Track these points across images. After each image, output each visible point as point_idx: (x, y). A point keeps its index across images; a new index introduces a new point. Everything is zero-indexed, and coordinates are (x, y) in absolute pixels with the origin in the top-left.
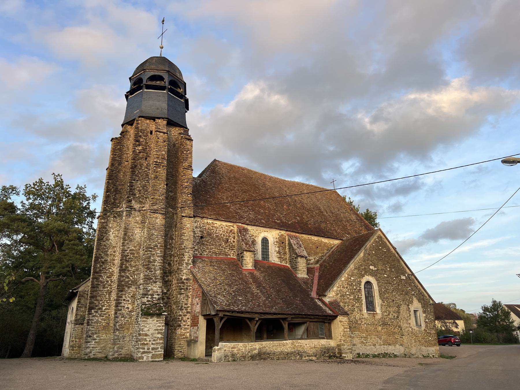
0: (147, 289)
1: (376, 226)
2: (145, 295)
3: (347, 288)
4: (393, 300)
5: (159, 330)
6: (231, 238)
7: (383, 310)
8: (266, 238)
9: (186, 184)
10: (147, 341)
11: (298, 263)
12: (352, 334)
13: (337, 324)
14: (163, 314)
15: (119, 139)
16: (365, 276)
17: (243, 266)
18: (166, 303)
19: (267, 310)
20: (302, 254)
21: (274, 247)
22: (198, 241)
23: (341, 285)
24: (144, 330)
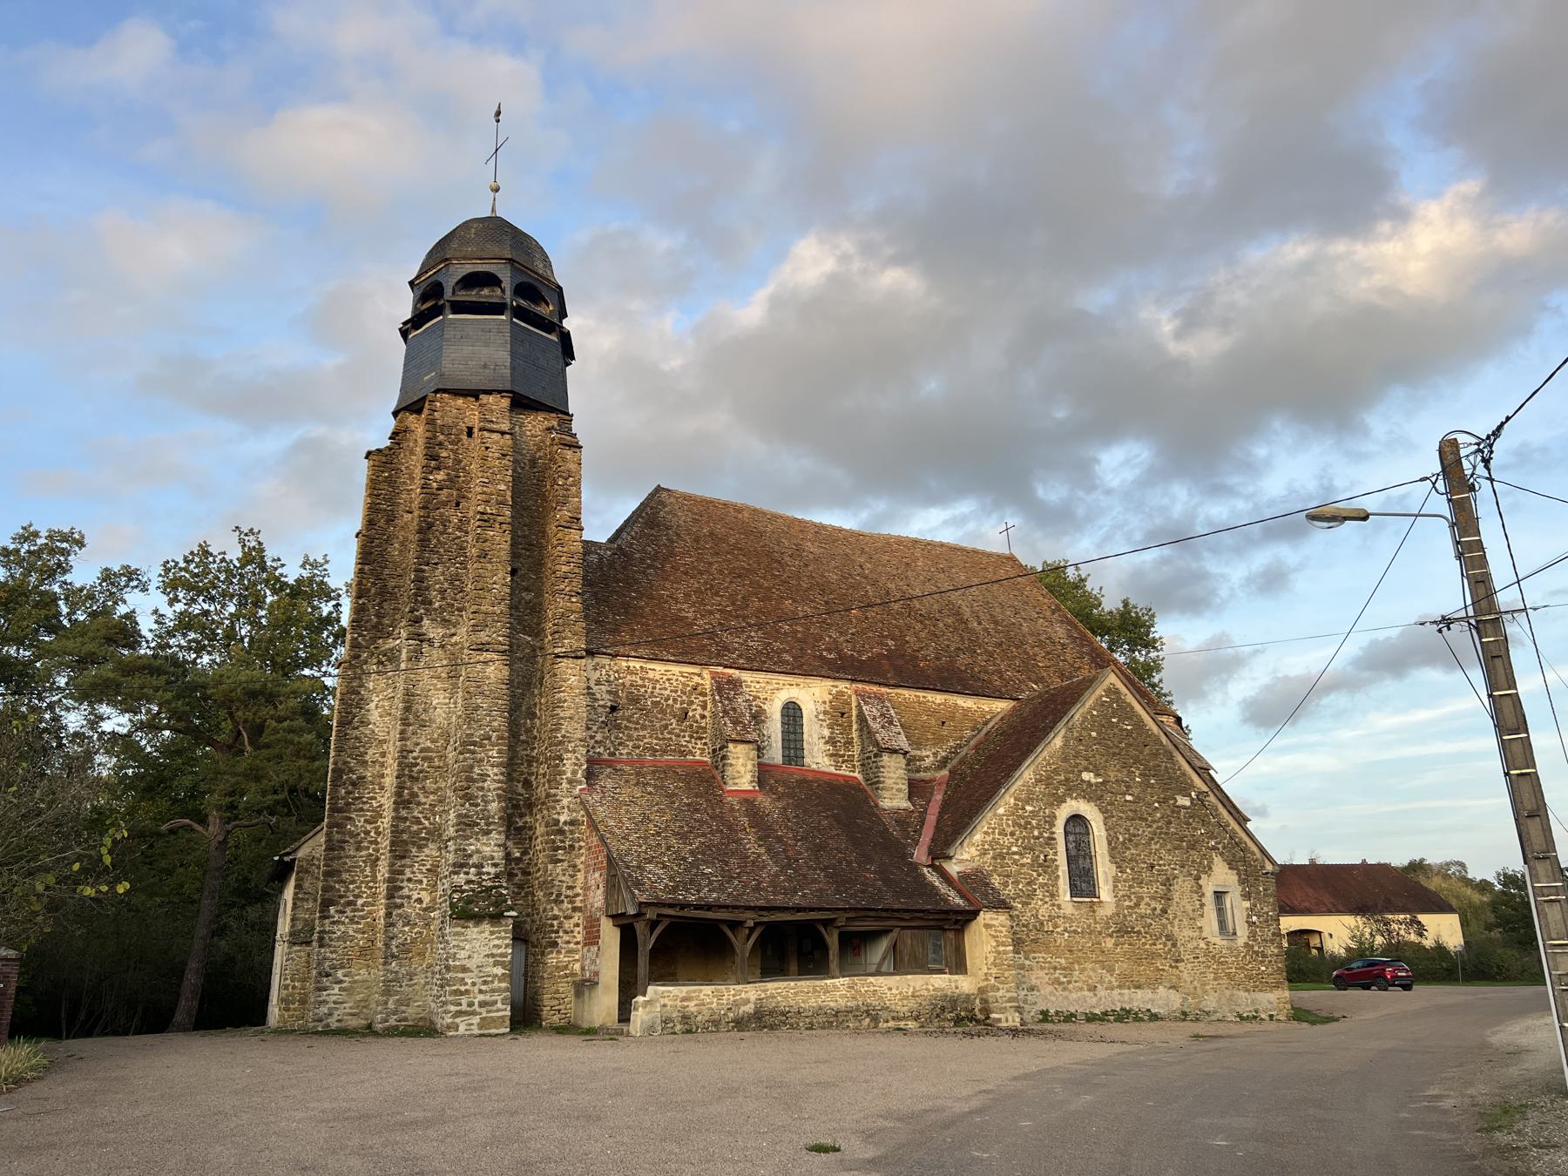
0: (465, 850)
1: (1154, 647)
2: (459, 866)
3: (1012, 834)
5: (497, 955)
7: (1121, 893)
9: (565, 569)
10: (466, 984)
11: (882, 770)
14: (505, 914)
15: (387, 452)
16: (1068, 800)
18: (520, 886)
19: (779, 900)
20: (895, 745)
21: (817, 726)
22: (603, 719)
24: (458, 956)
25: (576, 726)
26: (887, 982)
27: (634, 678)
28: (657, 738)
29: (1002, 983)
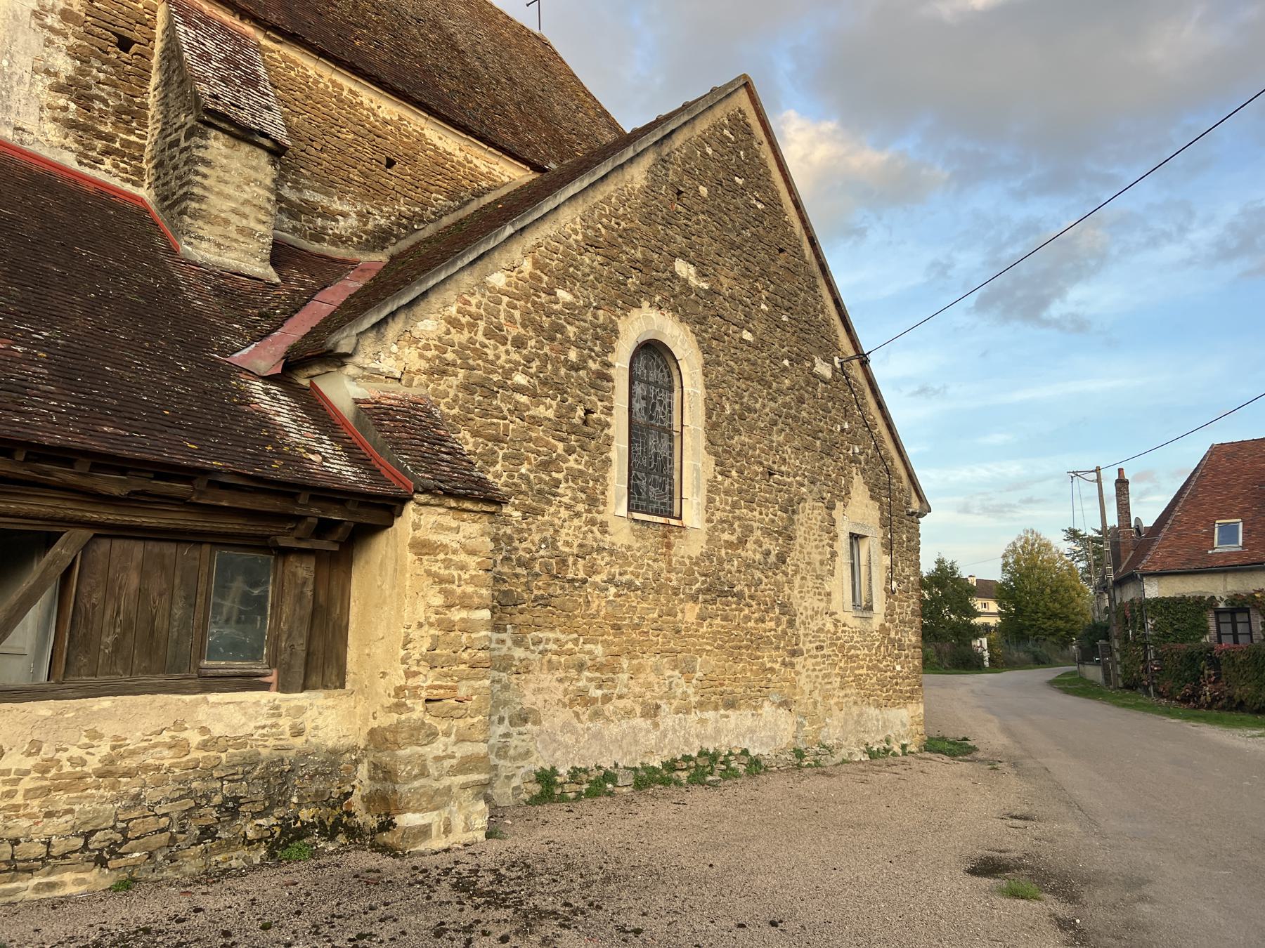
3: (519, 343)
4: (770, 468)
7: (719, 515)
11: (202, 169)
12: (518, 643)
13: (390, 566)
16: (645, 304)
23: (477, 318)
29: (447, 716)
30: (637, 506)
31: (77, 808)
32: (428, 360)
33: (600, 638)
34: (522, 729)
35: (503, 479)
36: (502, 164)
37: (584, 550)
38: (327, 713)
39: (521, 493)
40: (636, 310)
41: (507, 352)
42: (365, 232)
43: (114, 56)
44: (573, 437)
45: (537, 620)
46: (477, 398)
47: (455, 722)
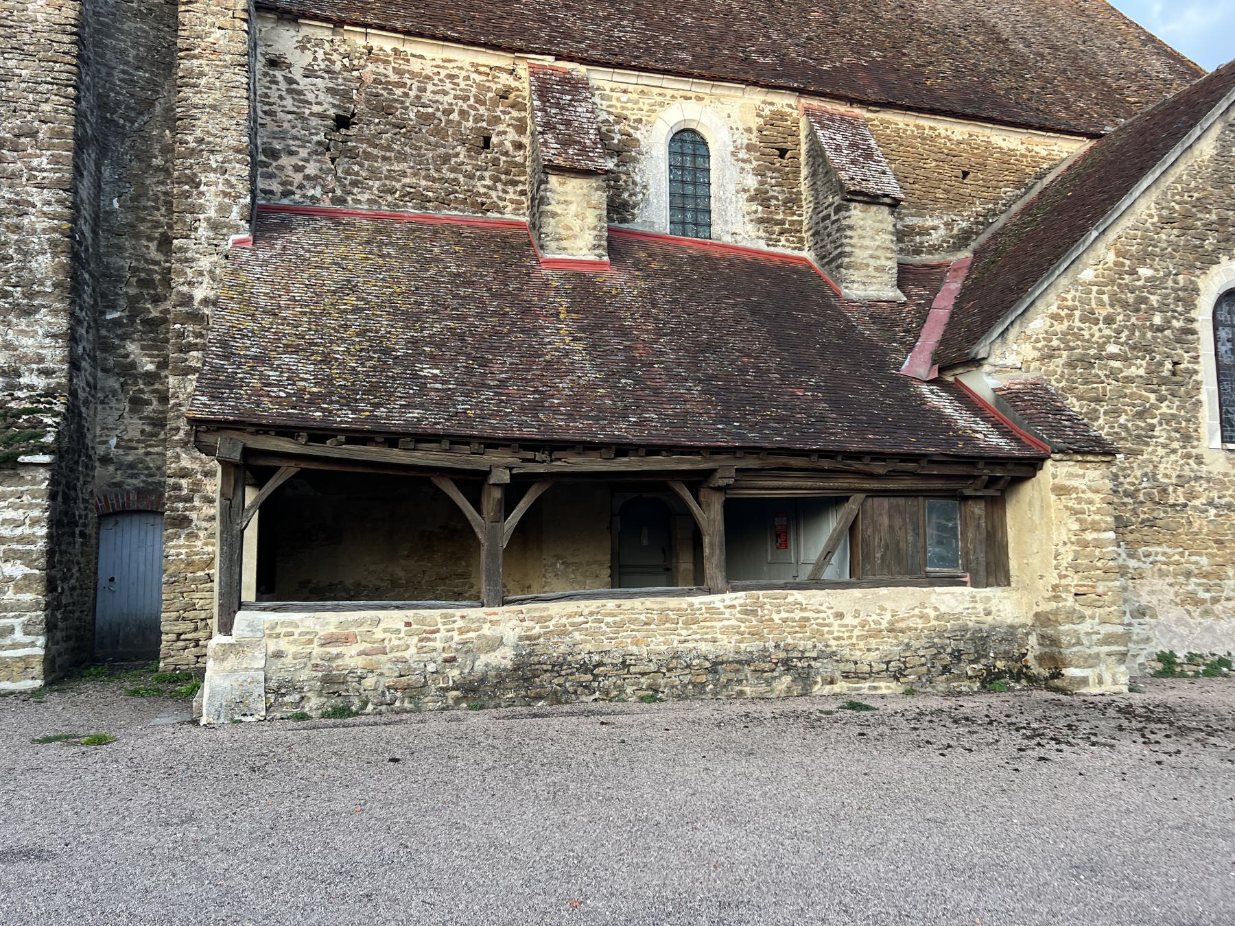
3: (1109, 320)
5: (11, 540)
6: (501, 128)
8: (693, 131)
11: (849, 233)
12: (1130, 556)
13: (1037, 504)
14: (24, 459)
16: (1224, 259)
17: (542, 247)
19: (579, 428)
20: (872, 188)
22: (321, 137)
25: (226, 122)
26: (830, 599)
27: (381, 69)
28: (427, 178)
30: (1231, 437)
31: (881, 647)
32: (1039, 350)
33: (1205, 551)
34: (1141, 621)
35: (1106, 430)
36: (1060, 143)
37: (1182, 479)
38: (1005, 601)
39: (1122, 439)
40: (1214, 266)
41: (1100, 330)
42: (951, 237)
43: (778, 165)
44: (1163, 387)
45: (1145, 538)
46: (1079, 370)
47: (1097, 610)
